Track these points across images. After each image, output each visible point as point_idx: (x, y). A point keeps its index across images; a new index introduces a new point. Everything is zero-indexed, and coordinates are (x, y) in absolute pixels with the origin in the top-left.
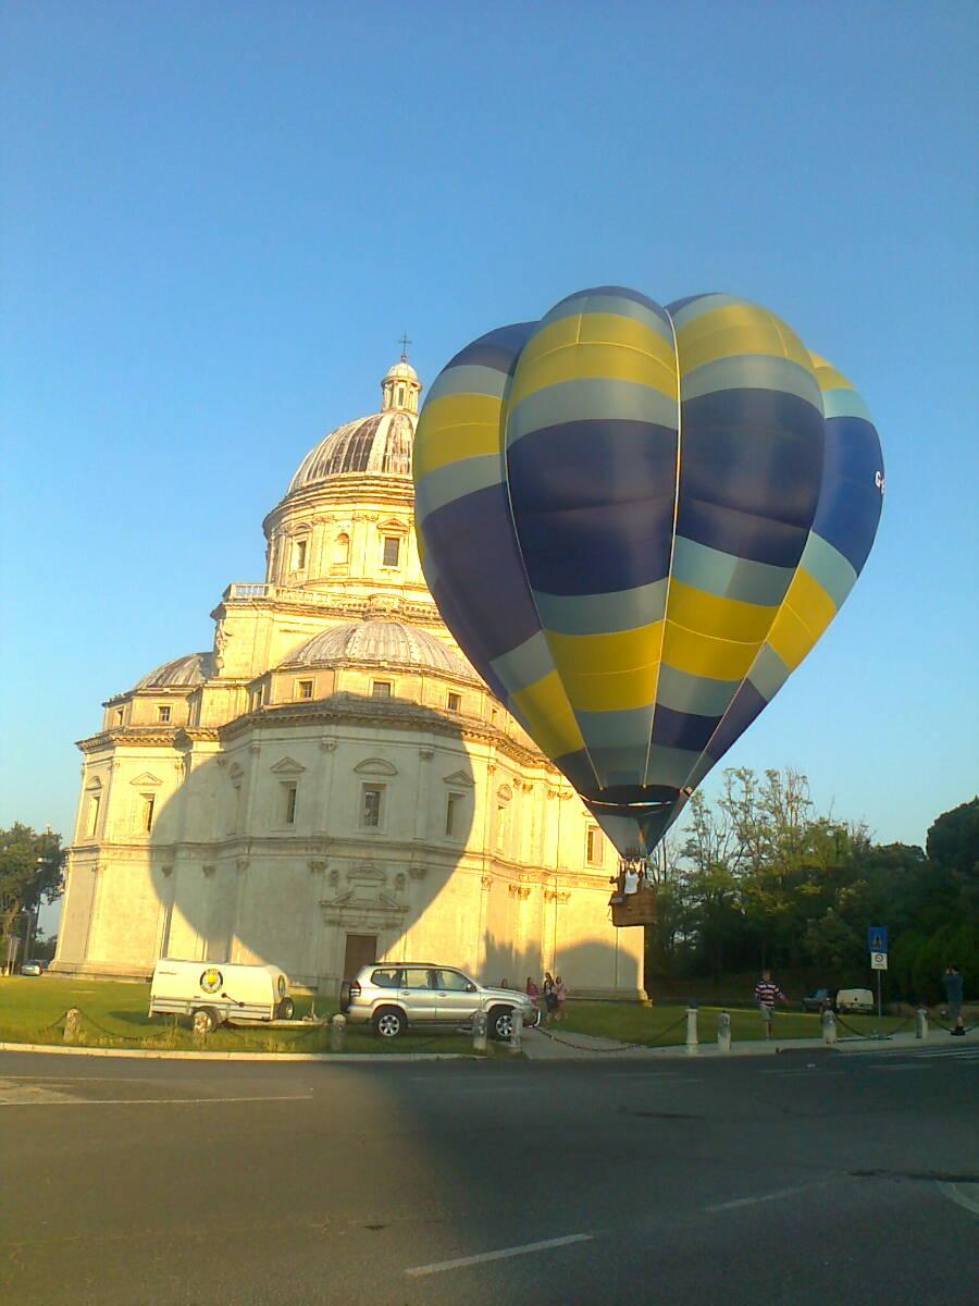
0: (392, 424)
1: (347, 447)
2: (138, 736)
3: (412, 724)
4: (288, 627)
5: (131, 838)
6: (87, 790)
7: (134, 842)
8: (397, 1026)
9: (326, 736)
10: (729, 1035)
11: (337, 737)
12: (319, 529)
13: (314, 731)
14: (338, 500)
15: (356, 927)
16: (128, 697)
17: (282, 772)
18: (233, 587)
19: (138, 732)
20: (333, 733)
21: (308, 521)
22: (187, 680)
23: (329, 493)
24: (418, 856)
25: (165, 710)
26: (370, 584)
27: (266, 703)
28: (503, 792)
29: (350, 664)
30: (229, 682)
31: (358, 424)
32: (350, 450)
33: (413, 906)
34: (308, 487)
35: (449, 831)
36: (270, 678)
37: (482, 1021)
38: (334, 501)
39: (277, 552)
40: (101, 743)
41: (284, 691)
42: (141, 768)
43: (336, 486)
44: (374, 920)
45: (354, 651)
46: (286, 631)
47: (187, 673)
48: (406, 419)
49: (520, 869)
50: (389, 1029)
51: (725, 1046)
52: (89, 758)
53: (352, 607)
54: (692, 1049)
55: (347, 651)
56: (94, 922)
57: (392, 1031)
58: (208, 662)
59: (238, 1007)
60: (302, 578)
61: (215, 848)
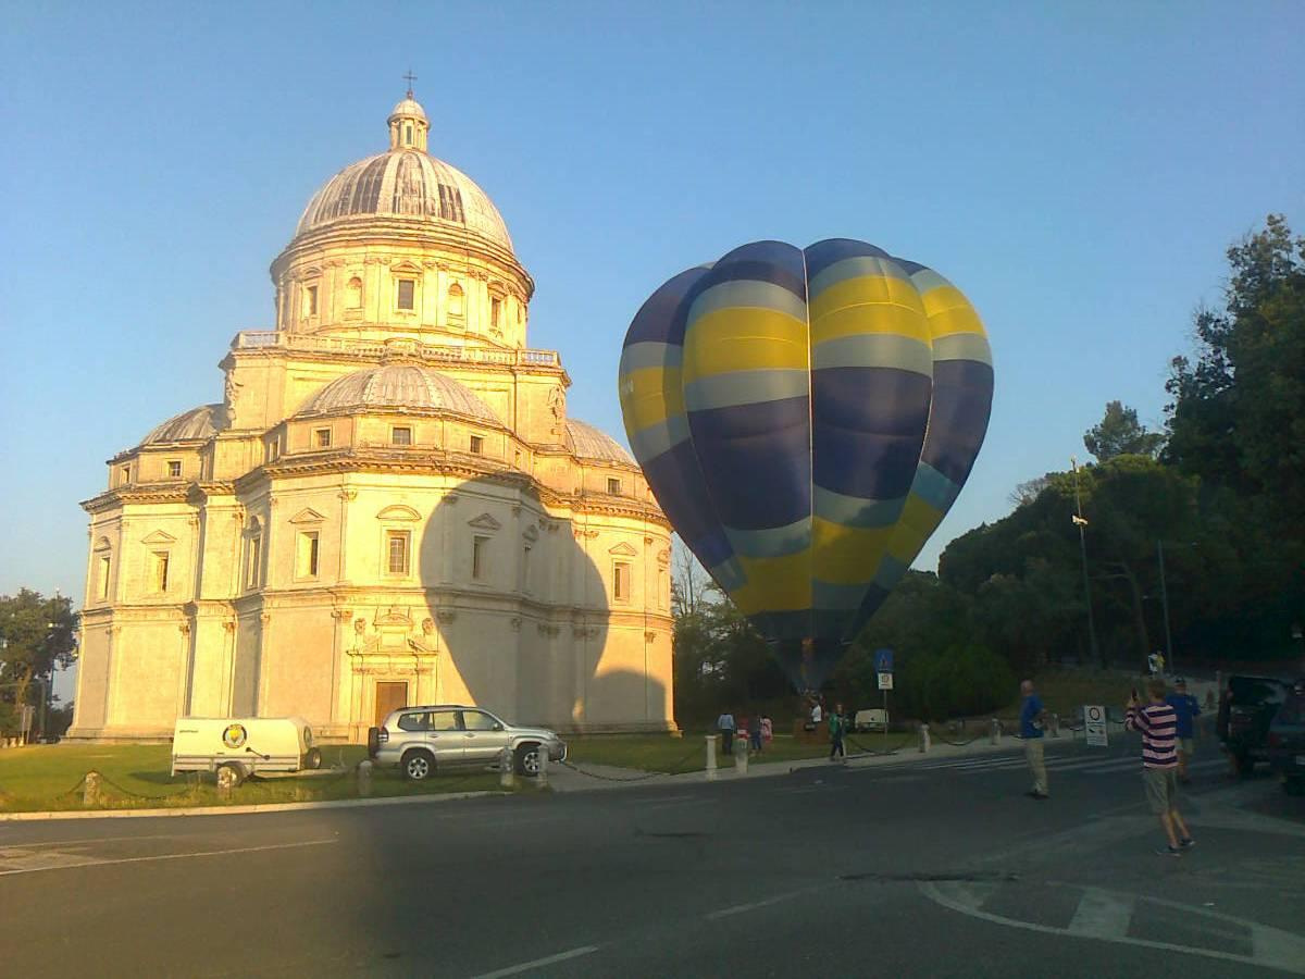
0: (401, 164)
1: (354, 188)
2: (146, 493)
4: (301, 374)
5: (148, 598)
6: (95, 551)
7: (149, 602)
8: (426, 768)
10: (746, 758)
12: (332, 271)
13: (335, 479)
14: (348, 243)
15: (383, 674)
16: (134, 454)
17: (303, 522)
18: (242, 336)
19: (147, 489)
21: (318, 265)
22: (198, 433)
23: (338, 236)
24: (445, 600)
25: (175, 465)
26: (387, 328)
27: (283, 453)
28: (530, 535)
29: (368, 410)
30: (243, 434)
31: (366, 164)
32: (358, 192)
34: (317, 229)
35: (475, 574)
36: (286, 427)
37: (509, 758)
38: (343, 244)
39: (287, 297)
40: (108, 502)
41: (300, 440)
42: (153, 526)
43: (345, 229)
44: (399, 667)
45: (371, 397)
47: (196, 426)
48: (414, 157)
49: (548, 610)
50: (418, 771)
51: (742, 768)
52: (95, 519)
53: (367, 353)
54: (712, 774)
55: (364, 398)
56: (111, 685)
57: (421, 773)
58: (219, 415)
59: (263, 761)
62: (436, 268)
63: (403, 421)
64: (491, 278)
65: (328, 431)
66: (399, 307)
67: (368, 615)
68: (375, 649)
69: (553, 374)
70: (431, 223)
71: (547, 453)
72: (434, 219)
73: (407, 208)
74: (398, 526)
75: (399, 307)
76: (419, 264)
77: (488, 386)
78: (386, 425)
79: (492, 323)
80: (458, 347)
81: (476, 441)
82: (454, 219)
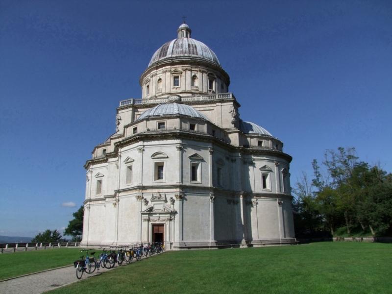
7: (97, 198)
9: (141, 145)
11: (144, 146)
14: (157, 68)
15: (155, 221)
20: (142, 144)
29: (148, 119)
33: (178, 211)
60: (149, 97)
61: (114, 196)
63: (161, 121)
64: (208, 73)
66: (174, 85)
67: (148, 198)
68: (150, 211)
69: (230, 101)
71: (230, 131)
72: (186, 55)
73: (176, 52)
81: (192, 127)
82: (194, 54)
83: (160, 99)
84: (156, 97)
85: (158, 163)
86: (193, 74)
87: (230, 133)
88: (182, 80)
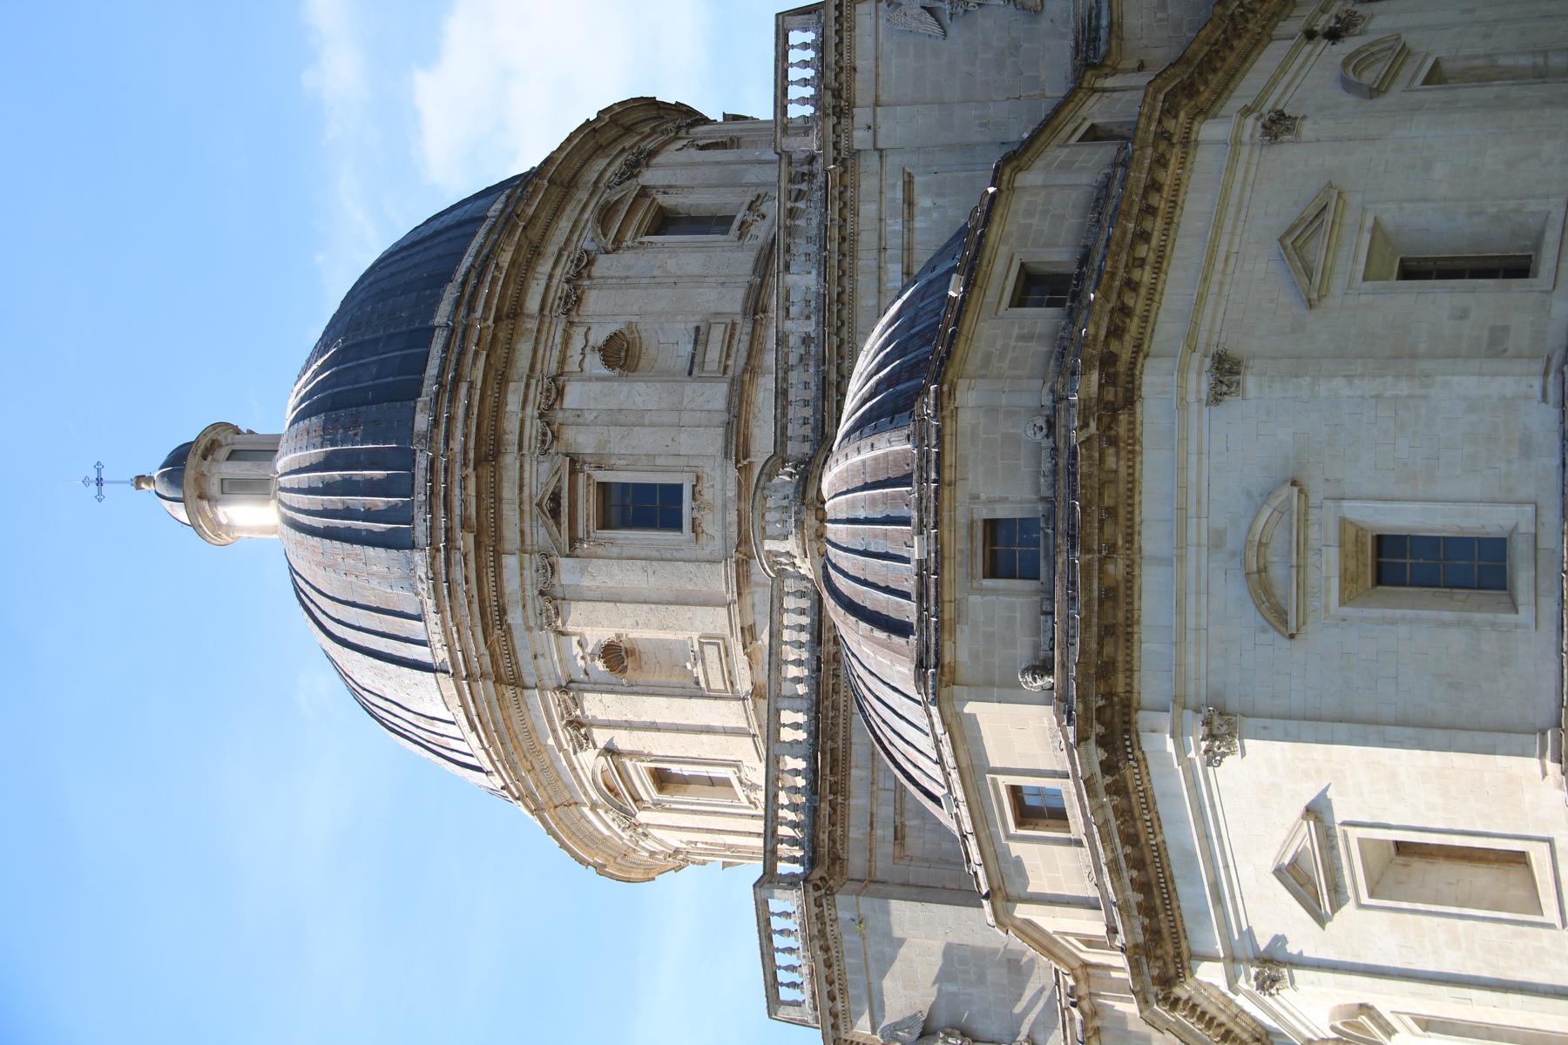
3: (1113, 442)
4: (884, 832)
35: (1517, 268)
46: (899, 835)
62: (559, 416)
63: (964, 547)
65: (1015, 791)
66: (677, 526)
70: (429, 437)
71: (1104, 22)
74: (1327, 566)
75: (677, 526)
76: (545, 467)
77: (894, 243)
78: (974, 599)
79: (726, 232)
80: (781, 341)
83: (775, 635)
84: (768, 695)
85: (1346, 578)
86: (594, 364)
87: (1115, 27)
88: (637, 459)
